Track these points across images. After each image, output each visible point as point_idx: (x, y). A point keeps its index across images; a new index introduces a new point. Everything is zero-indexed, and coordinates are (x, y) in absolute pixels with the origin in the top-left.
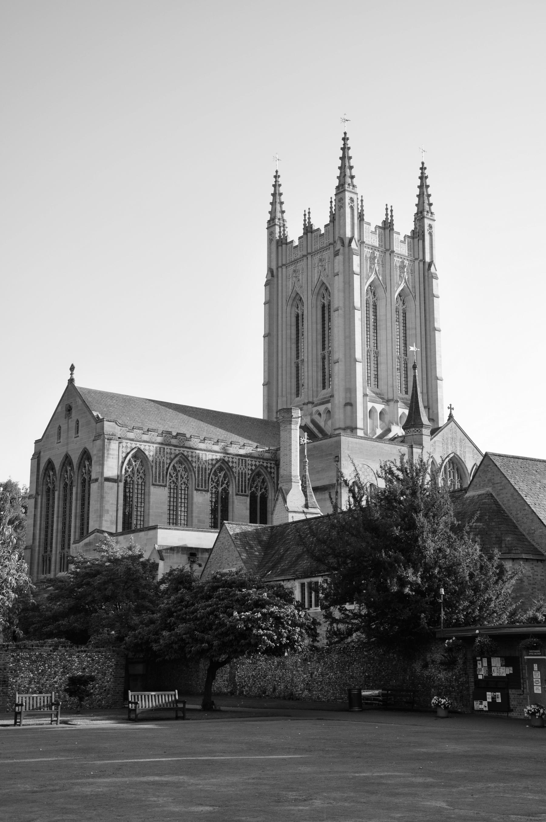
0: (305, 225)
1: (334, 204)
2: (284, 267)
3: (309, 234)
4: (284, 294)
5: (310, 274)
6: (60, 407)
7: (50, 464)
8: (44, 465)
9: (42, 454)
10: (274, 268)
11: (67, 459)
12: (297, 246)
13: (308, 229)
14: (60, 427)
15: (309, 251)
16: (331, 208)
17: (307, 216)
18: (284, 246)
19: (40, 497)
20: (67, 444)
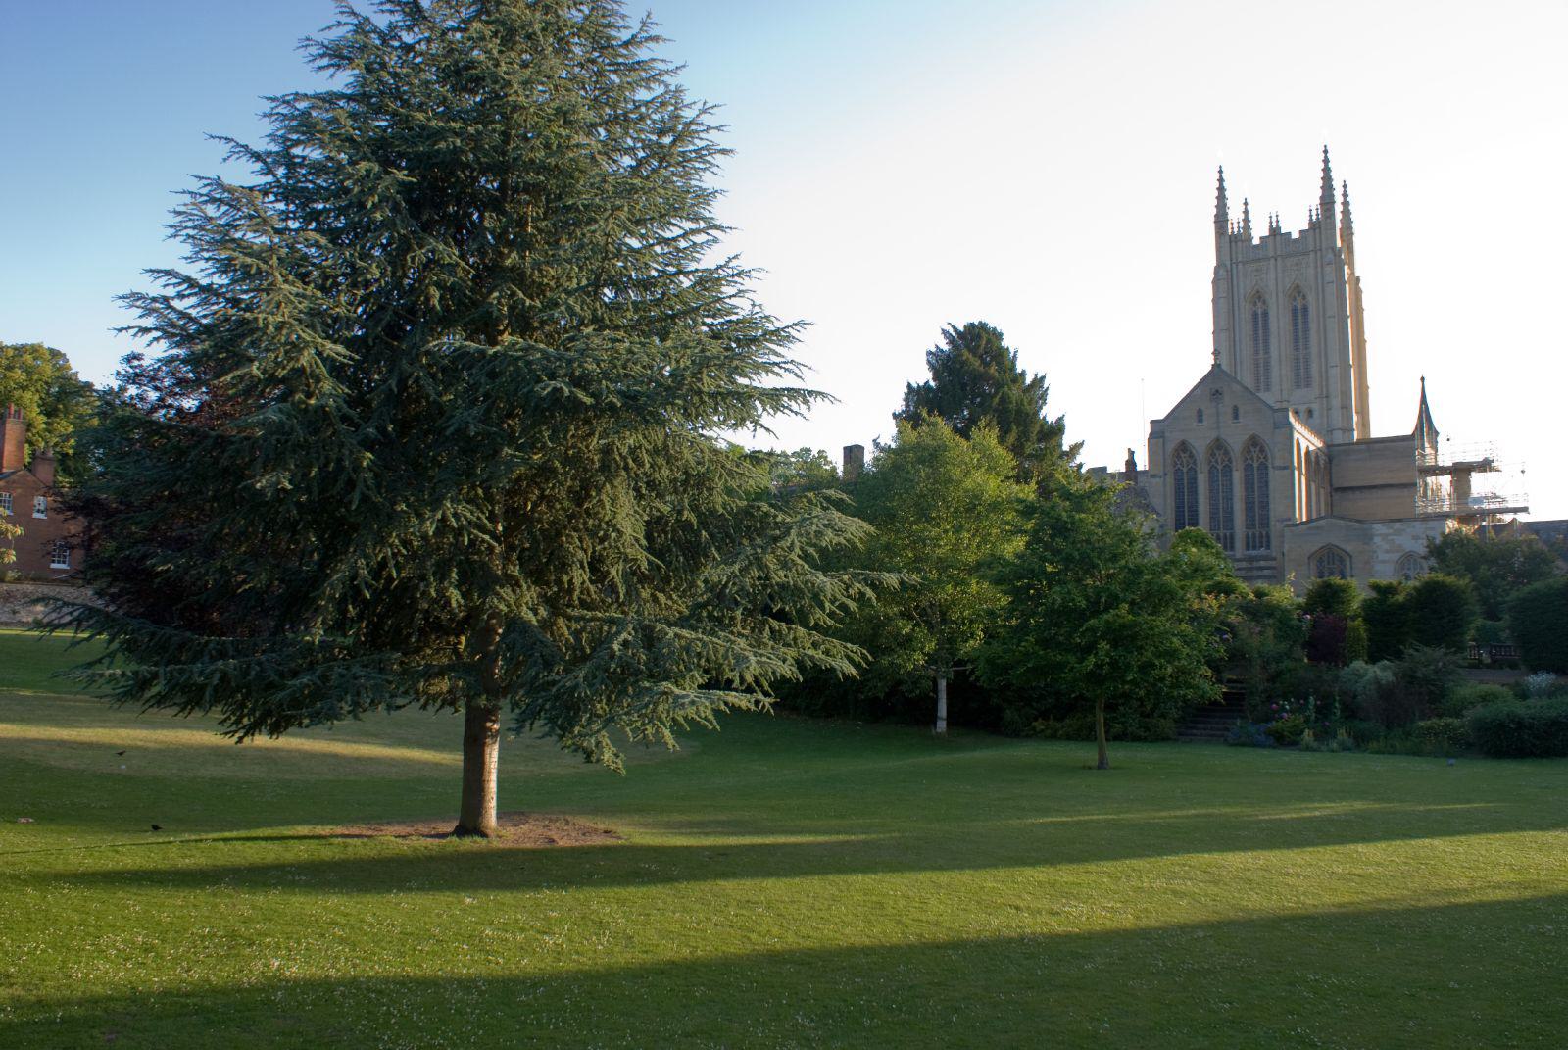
0: (1271, 226)
1: (1314, 213)
2: (1240, 266)
3: (1278, 238)
4: (1241, 291)
5: (1280, 275)
6: (1198, 391)
7: (1183, 447)
8: (1173, 446)
9: (1167, 435)
10: (1228, 263)
11: (1218, 446)
12: (1257, 246)
13: (1275, 231)
14: (1200, 413)
15: (1279, 253)
16: (1311, 216)
17: (1274, 219)
18: (1239, 244)
19: (1168, 477)
20: (1218, 428)
